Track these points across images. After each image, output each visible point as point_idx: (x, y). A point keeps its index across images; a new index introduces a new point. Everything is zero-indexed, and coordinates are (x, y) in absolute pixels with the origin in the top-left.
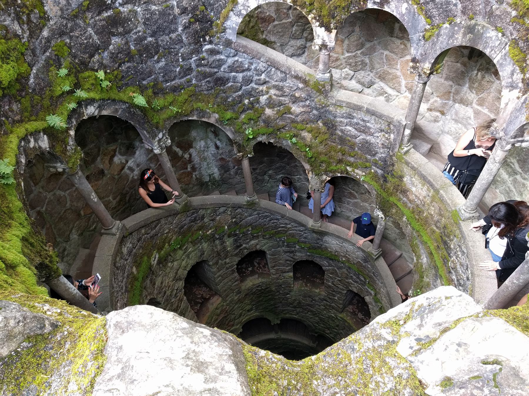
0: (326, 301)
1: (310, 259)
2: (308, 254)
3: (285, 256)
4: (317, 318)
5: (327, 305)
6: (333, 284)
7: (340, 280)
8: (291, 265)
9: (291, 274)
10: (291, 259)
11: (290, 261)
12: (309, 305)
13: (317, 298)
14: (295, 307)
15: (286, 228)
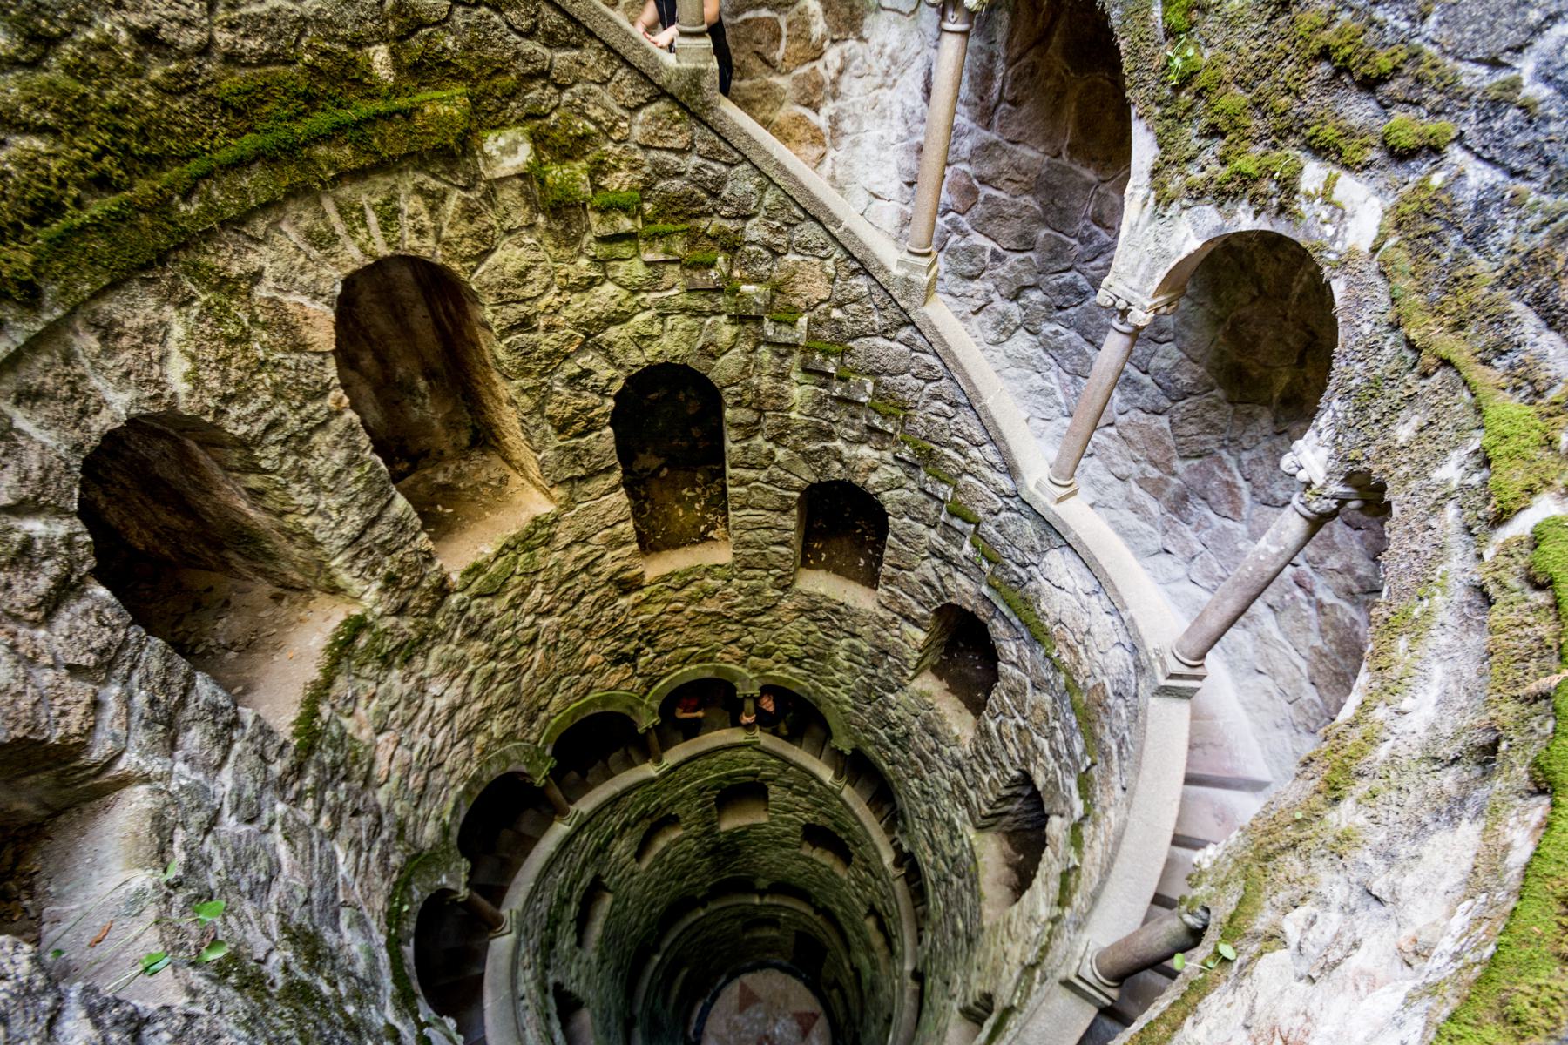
0: (962, 772)
1: (982, 612)
2: (984, 589)
3: (928, 568)
4: (925, 807)
5: (958, 784)
6: (999, 731)
7: (1018, 727)
8: (930, 603)
9: (921, 636)
10: (938, 584)
11: (932, 587)
12: (922, 756)
13: (947, 751)
14: (894, 740)
15: (965, 457)
